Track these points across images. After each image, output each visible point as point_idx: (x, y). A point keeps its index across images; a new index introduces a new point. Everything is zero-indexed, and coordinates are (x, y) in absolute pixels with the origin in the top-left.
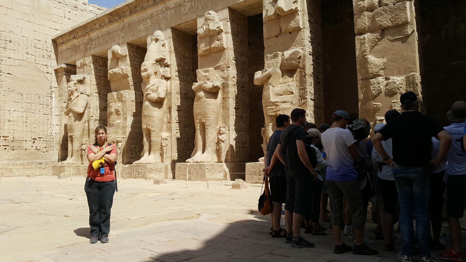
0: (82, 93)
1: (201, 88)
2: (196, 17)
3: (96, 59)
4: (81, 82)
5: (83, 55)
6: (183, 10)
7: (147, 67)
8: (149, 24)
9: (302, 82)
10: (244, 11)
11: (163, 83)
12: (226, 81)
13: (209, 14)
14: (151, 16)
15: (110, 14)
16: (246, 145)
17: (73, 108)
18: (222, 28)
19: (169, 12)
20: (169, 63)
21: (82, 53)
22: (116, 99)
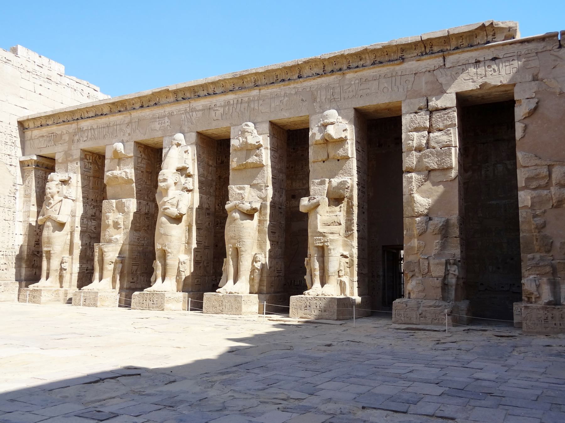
0: (66, 197)
1: (236, 208)
2: (229, 125)
3: (86, 155)
4: (64, 182)
5: (67, 147)
6: (214, 115)
7: (167, 177)
8: (167, 124)
9: (349, 212)
10: (285, 126)
11: (181, 194)
12: (264, 201)
13: (247, 125)
14: (171, 115)
15: (113, 104)
16: (281, 274)
17: (54, 215)
18: (261, 143)
19: (194, 113)
20: (192, 173)
21: (65, 144)
22: (115, 209)
